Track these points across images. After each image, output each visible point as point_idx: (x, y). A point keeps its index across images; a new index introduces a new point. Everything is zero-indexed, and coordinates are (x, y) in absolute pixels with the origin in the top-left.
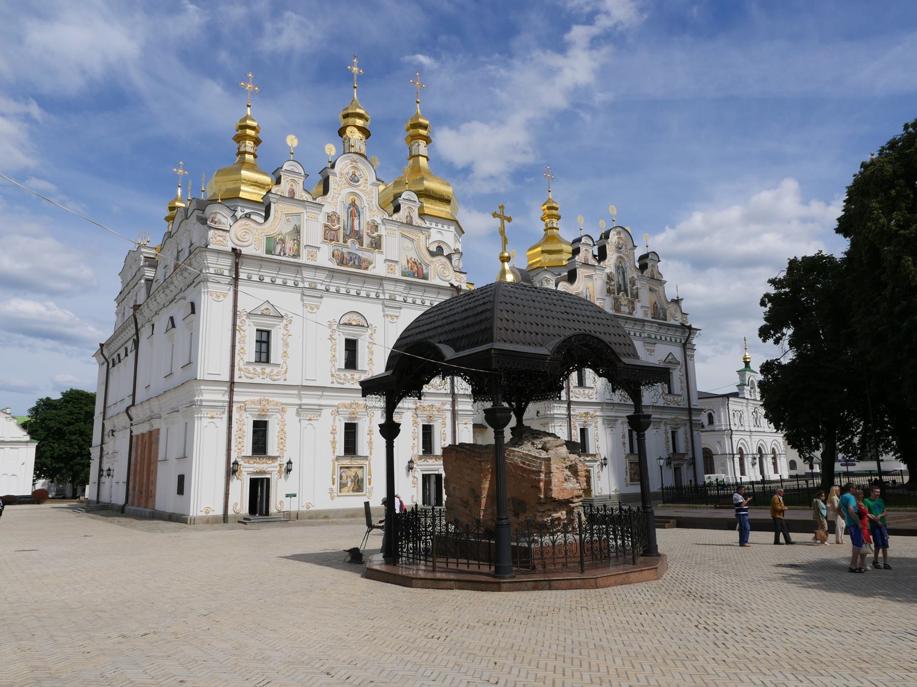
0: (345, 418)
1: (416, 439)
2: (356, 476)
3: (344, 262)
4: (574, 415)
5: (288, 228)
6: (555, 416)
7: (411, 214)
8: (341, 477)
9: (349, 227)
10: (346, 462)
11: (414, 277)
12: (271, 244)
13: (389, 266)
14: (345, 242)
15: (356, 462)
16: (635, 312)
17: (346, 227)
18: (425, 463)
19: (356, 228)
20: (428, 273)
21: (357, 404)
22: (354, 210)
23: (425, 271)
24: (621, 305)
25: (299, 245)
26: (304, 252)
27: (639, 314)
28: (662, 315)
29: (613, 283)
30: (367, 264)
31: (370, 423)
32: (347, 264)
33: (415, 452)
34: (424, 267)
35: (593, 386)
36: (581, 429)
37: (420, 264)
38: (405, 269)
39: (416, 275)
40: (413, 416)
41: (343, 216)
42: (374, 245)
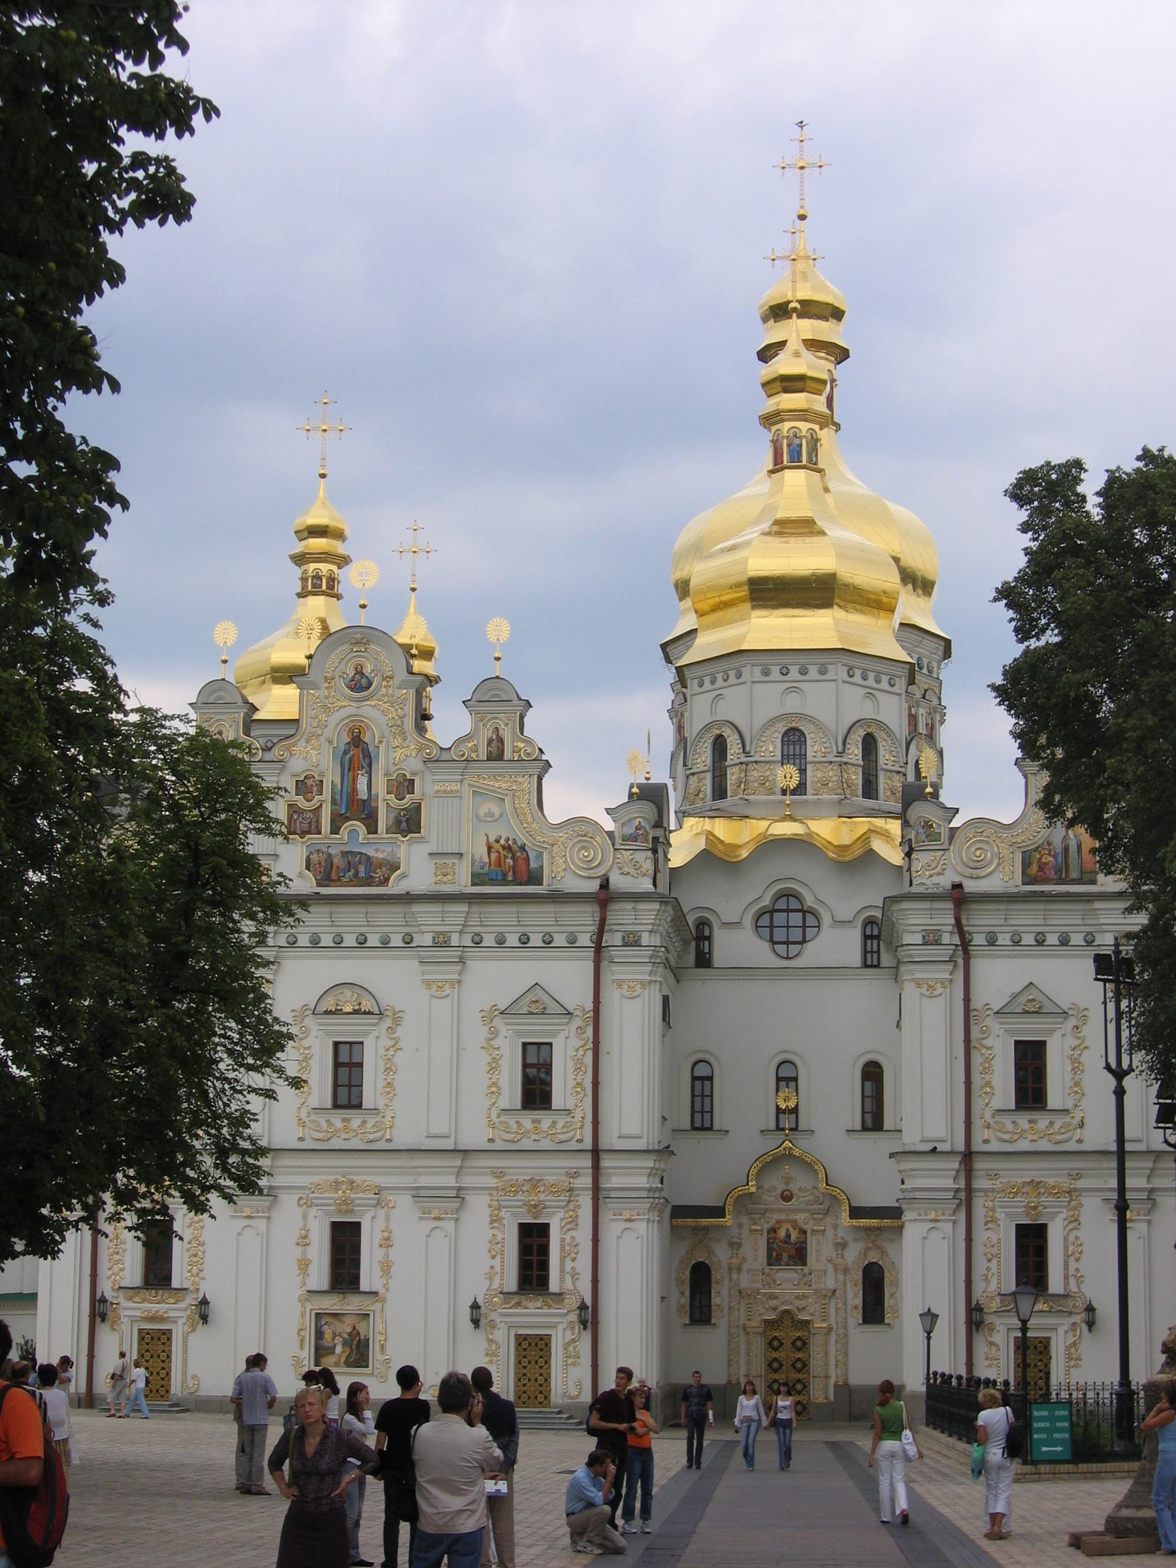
0: (327, 1213)
1: (499, 1257)
2: (354, 1333)
3: (334, 876)
4: (993, 1190)
6: (918, 1195)
7: (501, 732)
8: (319, 1334)
9: (345, 796)
10: (332, 1303)
11: (504, 882)
14: (335, 830)
15: (352, 1304)
17: (338, 797)
18: (519, 1310)
20: (542, 867)
21: (352, 1182)
23: (533, 865)
31: (387, 1219)
32: (339, 880)
33: (496, 1285)
35: (1069, 1105)
36: (1023, 1232)
37: (523, 848)
38: (482, 868)
39: (510, 878)
40: (490, 1206)
41: (332, 776)
42: (404, 825)
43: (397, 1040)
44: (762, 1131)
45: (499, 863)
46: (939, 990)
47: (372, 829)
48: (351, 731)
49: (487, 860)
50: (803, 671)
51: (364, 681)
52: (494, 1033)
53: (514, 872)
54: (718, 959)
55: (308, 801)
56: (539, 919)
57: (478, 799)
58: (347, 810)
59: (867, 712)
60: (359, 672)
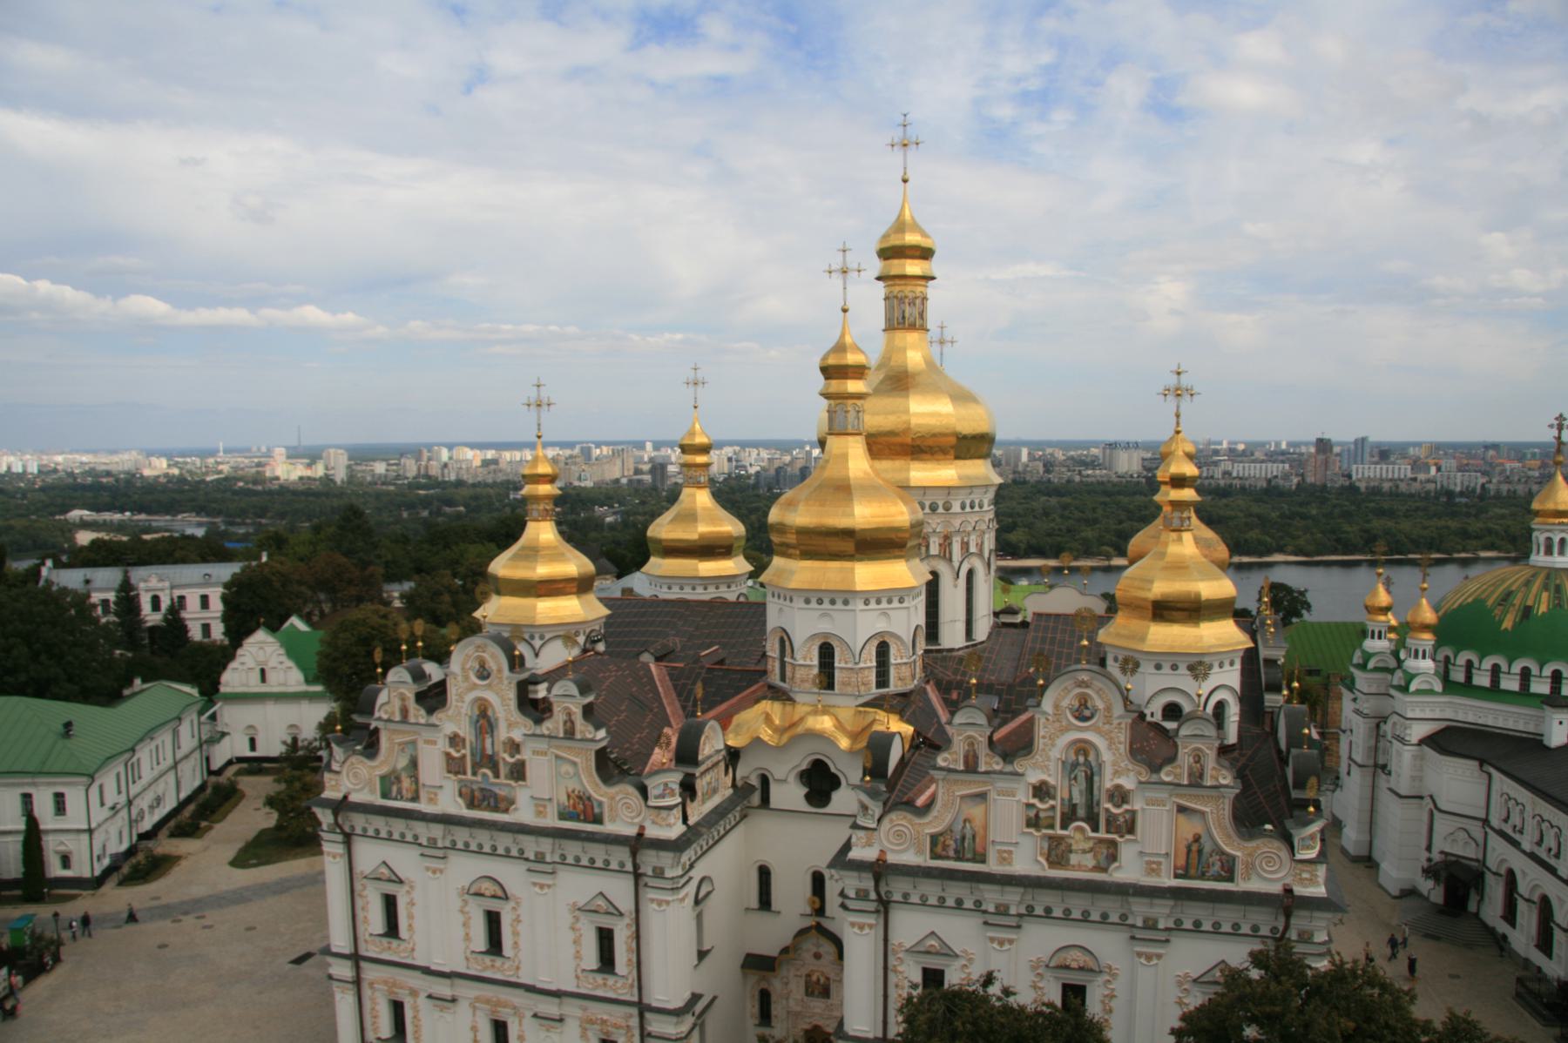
3: (476, 803)
5: (403, 762)
12: (388, 784)
13: (536, 805)
14: (474, 774)
16: (1116, 864)
19: (489, 752)
22: (484, 720)
23: (597, 810)
24: (1071, 851)
25: (417, 781)
26: (423, 794)
27: (1128, 870)
28: (1217, 868)
29: (1052, 802)
30: (504, 804)
34: (595, 804)
37: (589, 798)
39: (582, 817)
42: (515, 775)
43: (518, 916)
44: (802, 915)
45: (574, 807)
46: (867, 930)
47: (497, 775)
48: (479, 708)
49: (567, 804)
50: (833, 602)
51: (485, 673)
52: (577, 919)
53: (585, 815)
54: (774, 802)
55: (458, 751)
56: (598, 852)
57: (559, 762)
58: (481, 760)
59: (881, 626)
60: (482, 665)
